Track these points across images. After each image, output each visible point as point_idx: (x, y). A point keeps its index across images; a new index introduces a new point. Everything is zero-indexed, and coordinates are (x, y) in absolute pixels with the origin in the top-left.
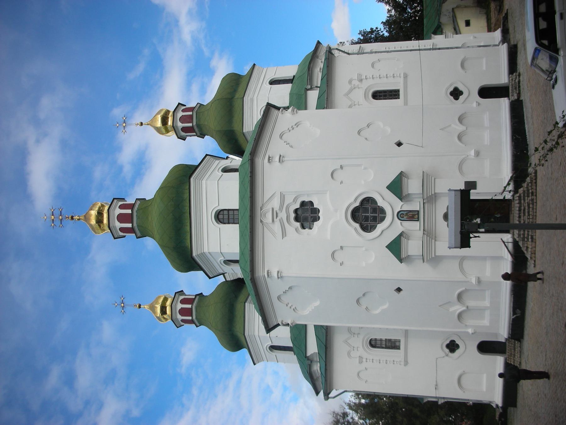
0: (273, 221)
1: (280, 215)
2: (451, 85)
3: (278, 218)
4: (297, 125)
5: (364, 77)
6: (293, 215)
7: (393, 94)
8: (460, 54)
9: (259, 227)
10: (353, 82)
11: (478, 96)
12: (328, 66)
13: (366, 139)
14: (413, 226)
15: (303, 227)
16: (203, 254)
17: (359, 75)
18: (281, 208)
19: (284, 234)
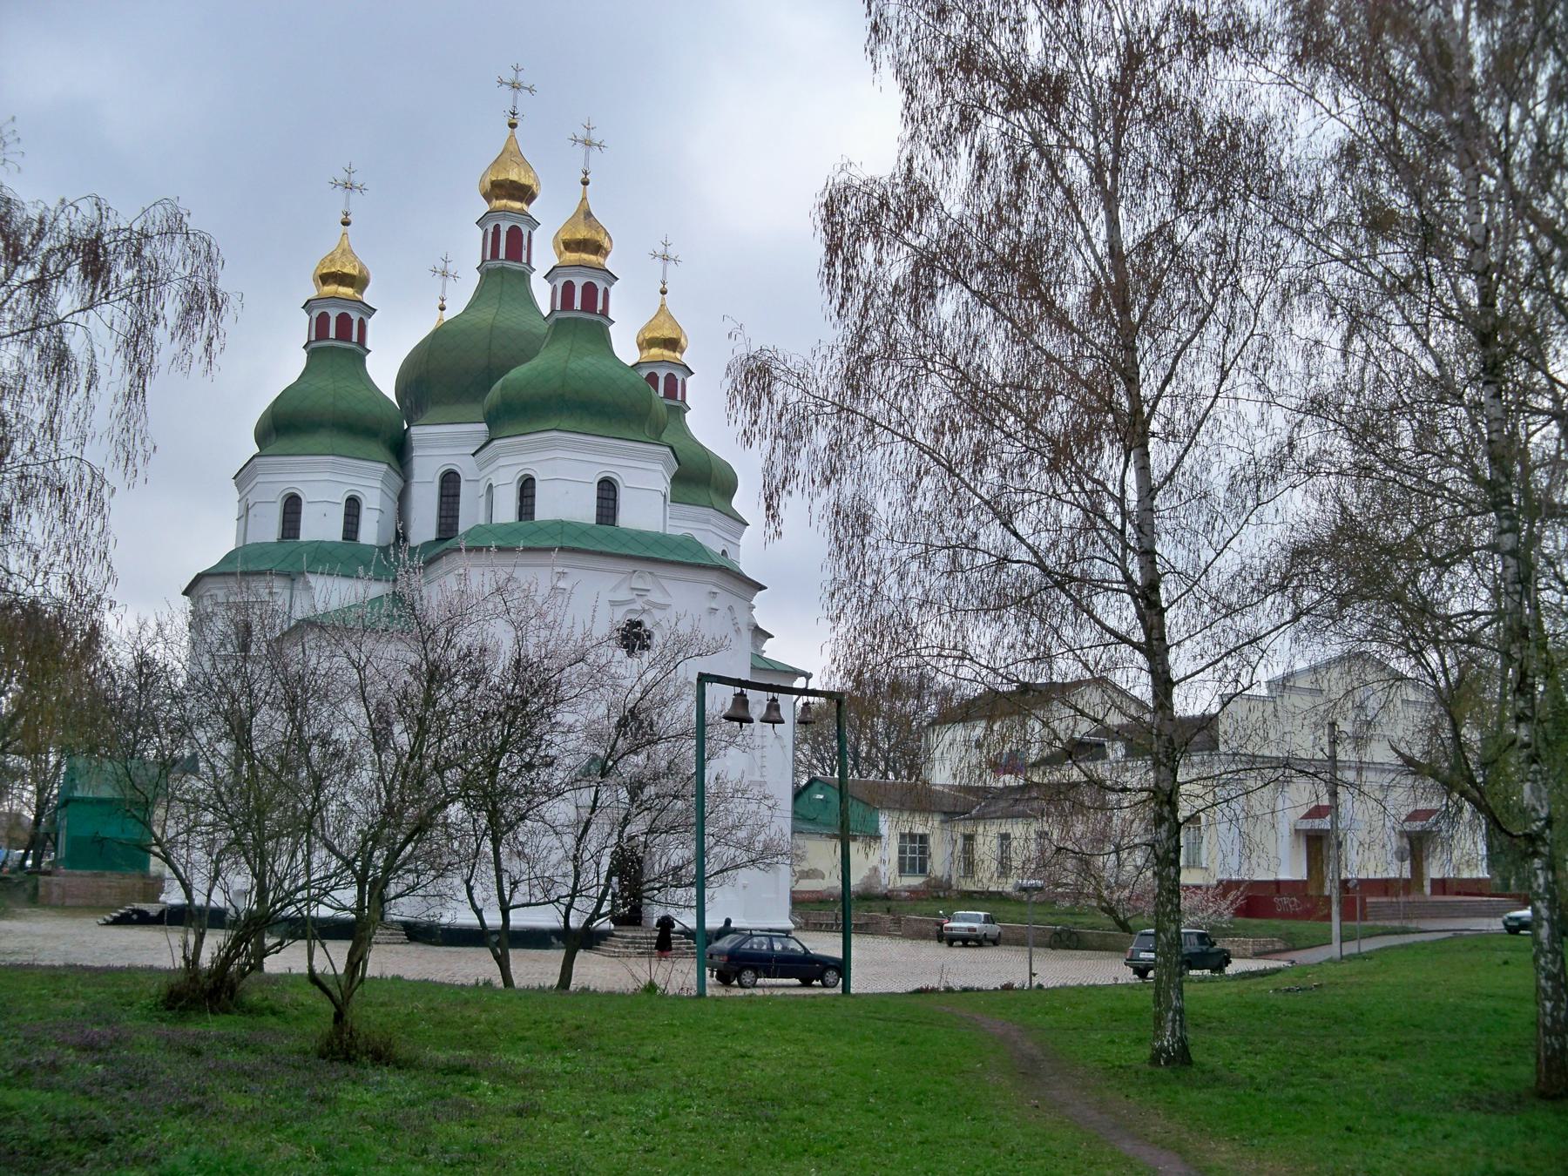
6: (634, 617)
9: (629, 566)
18: (648, 602)
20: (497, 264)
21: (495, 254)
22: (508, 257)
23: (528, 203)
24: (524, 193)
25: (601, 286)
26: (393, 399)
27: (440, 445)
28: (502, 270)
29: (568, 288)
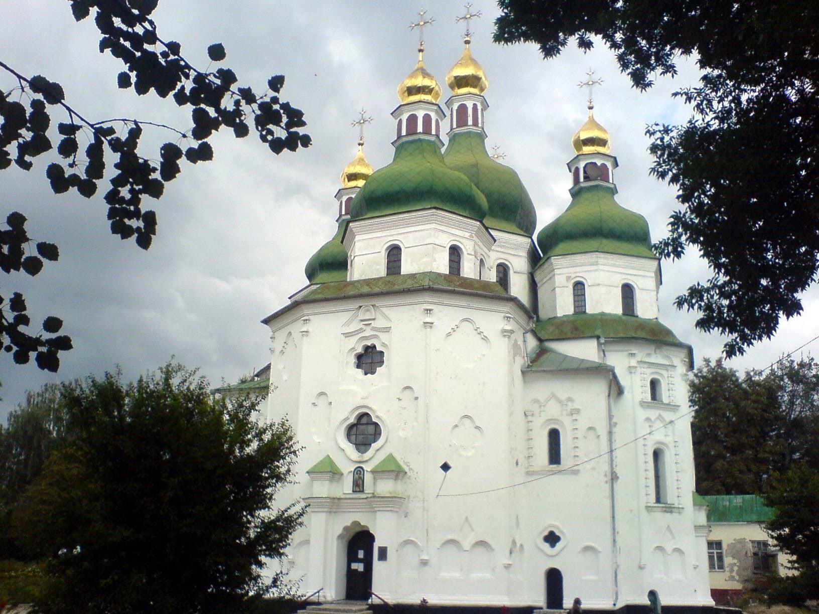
0: (362, 321)
1: (368, 328)
2: (562, 532)
3: (364, 327)
4: (485, 339)
5: (575, 417)
7: (555, 456)
8: (603, 544)
10: (570, 404)
11: (555, 567)
12: (567, 370)
13: (456, 426)
14: (347, 485)
15: (359, 357)
17: (578, 411)
18: (374, 329)
19: (347, 335)
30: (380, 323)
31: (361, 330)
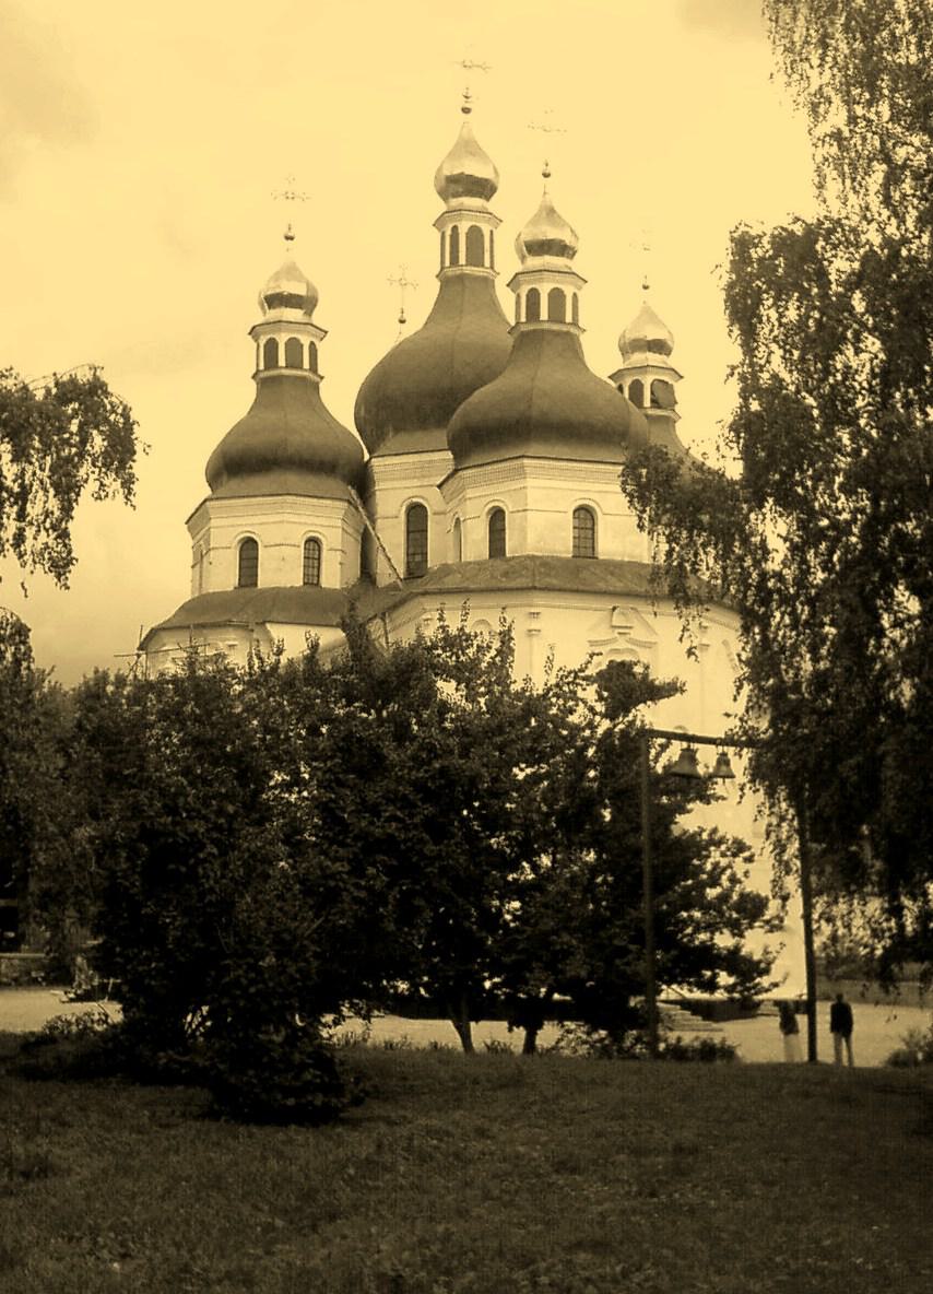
1: (622, 639)
16: (521, 473)
18: (632, 641)
20: (456, 271)
21: (454, 261)
22: (469, 263)
23: (488, 198)
24: (484, 188)
25: (569, 291)
26: (350, 424)
27: (405, 477)
28: (461, 278)
29: (533, 296)
30: (638, 633)
31: (614, 640)
